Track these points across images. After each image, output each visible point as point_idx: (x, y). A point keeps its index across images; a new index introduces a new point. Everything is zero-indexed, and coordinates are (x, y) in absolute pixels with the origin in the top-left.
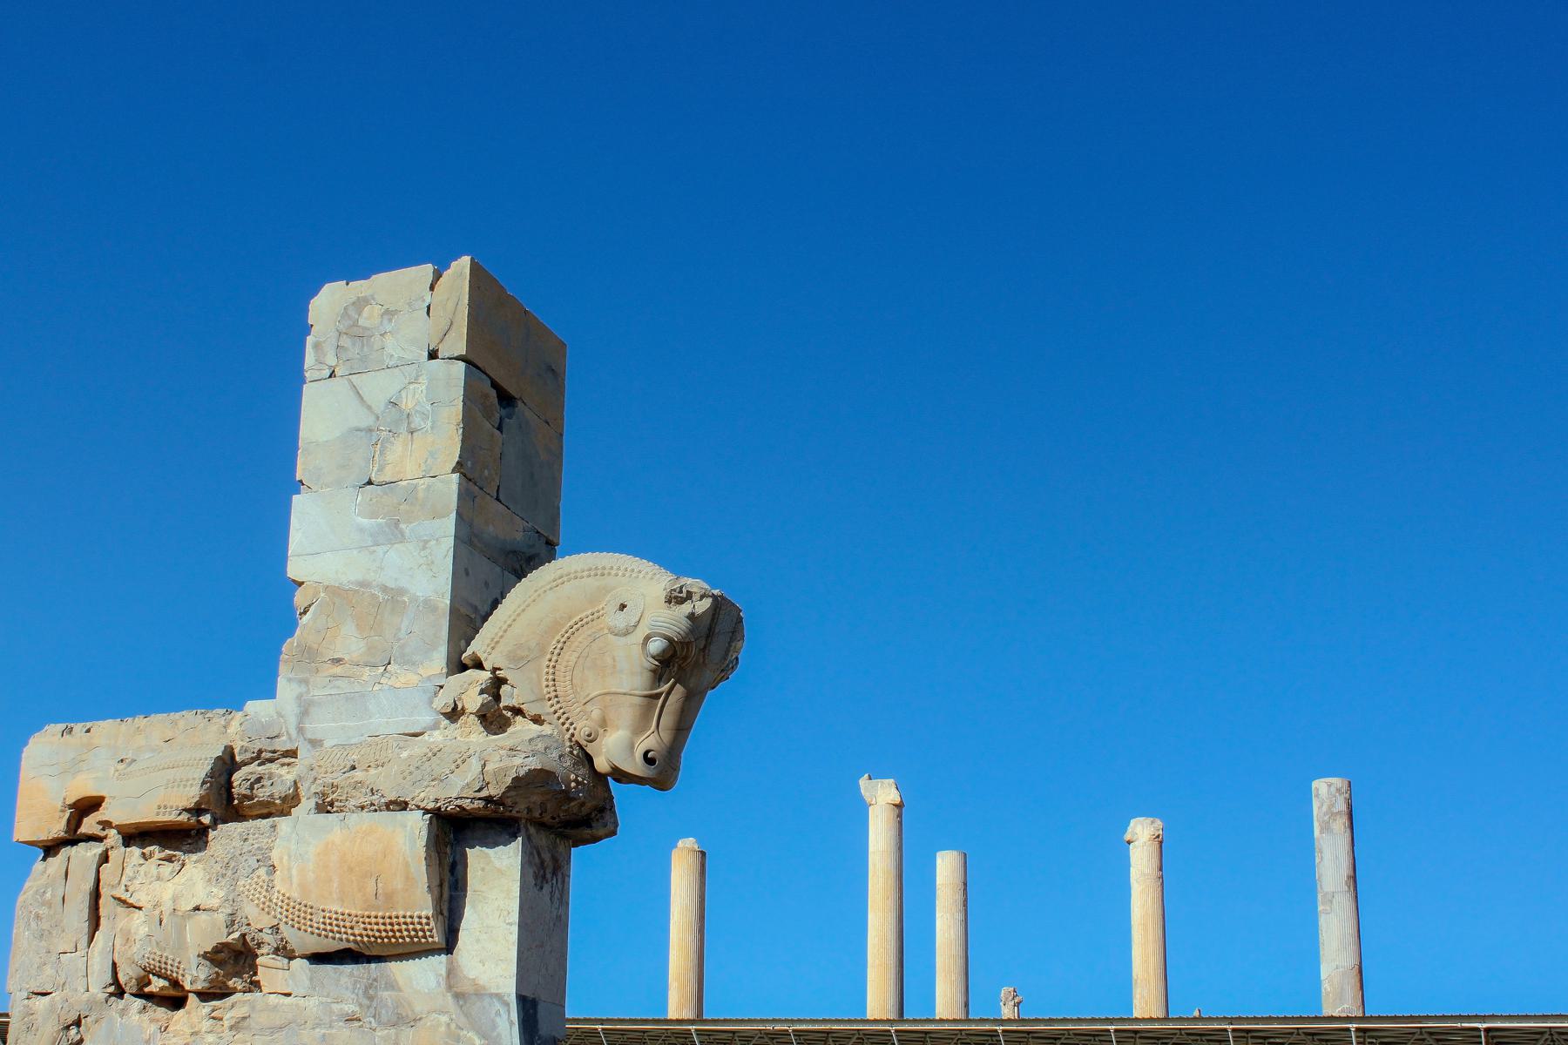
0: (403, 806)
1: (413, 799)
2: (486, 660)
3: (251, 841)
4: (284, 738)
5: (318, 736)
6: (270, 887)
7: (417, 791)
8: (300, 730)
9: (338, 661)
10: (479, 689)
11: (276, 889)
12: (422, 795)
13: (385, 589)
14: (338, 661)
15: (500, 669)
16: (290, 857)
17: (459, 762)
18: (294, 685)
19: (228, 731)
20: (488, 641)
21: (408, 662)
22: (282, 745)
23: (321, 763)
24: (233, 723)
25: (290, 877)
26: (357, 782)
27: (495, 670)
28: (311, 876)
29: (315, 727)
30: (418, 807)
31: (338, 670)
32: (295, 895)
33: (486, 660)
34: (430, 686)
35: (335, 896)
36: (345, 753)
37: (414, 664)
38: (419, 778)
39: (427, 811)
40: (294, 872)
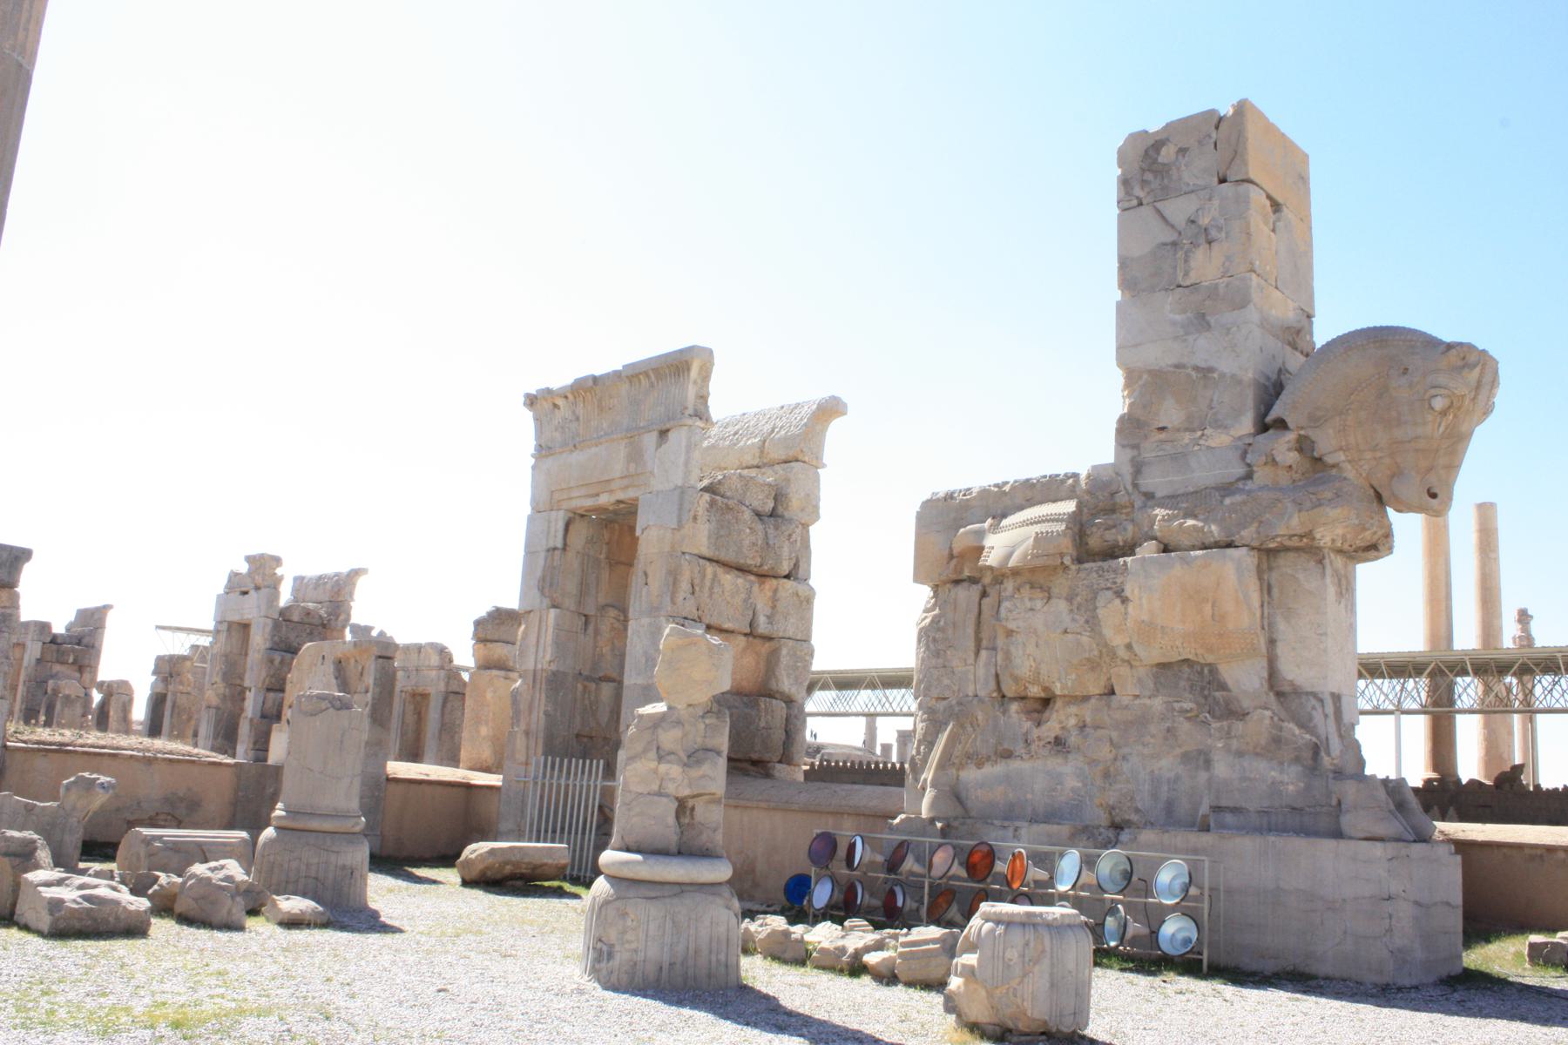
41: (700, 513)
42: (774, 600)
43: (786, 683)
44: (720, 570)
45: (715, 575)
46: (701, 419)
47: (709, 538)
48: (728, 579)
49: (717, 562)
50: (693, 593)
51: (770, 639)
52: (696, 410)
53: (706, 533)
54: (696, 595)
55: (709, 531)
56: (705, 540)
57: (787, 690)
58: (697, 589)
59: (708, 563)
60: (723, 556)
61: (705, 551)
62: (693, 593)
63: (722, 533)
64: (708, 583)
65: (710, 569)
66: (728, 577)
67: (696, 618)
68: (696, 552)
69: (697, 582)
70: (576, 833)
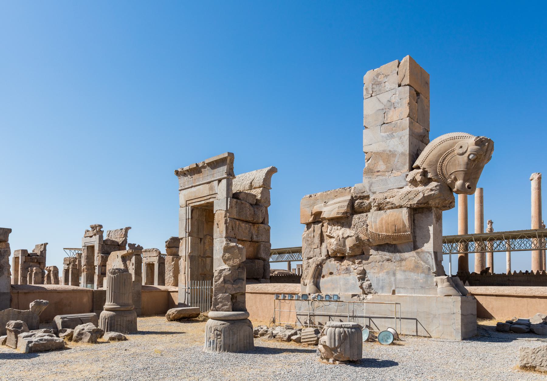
0: (401, 207)
1: (404, 205)
2: (421, 166)
3: (361, 219)
4: (366, 192)
5: (375, 191)
6: (367, 230)
7: (405, 203)
8: (370, 190)
9: (378, 171)
10: (420, 174)
11: (368, 230)
12: (406, 204)
13: (390, 151)
14: (378, 171)
15: (425, 168)
16: (372, 222)
17: (416, 194)
18: (367, 179)
19: (351, 192)
20: (421, 161)
21: (398, 170)
22: (365, 194)
23: (377, 198)
24: (352, 190)
25: (372, 227)
26: (387, 202)
27: (424, 169)
28: (378, 226)
29: (374, 189)
30: (405, 207)
31: (379, 174)
32: (373, 231)
33: (421, 166)
34: (405, 175)
35: (384, 231)
36: (383, 195)
37: (399, 170)
38: (405, 199)
39: (408, 208)
40: (373, 226)
41: (233, 205)
42: (258, 230)
43: (263, 254)
44: (241, 222)
45: (239, 224)
46: (231, 176)
47: (237, 213)
48: (243, 225)
49: (240, 220)
50: (233, 230)
51: (258, 242)
52: (229, 173)
53: (235, 211)
54: (234, 230)
55: (236, 210)
56: (235, 213)
57: (263, 257)
58: (234, 228)
59: (237, 221)
60: (241, 218)
61: (235, 217)
62: (233, 230)
63: (241, 211)
64: (237, 227)
65: (237, 222)
66: (243, 224)
67: (234, 237)
68: (233, 217)
69: (234, 226)
70: (204, 303)
